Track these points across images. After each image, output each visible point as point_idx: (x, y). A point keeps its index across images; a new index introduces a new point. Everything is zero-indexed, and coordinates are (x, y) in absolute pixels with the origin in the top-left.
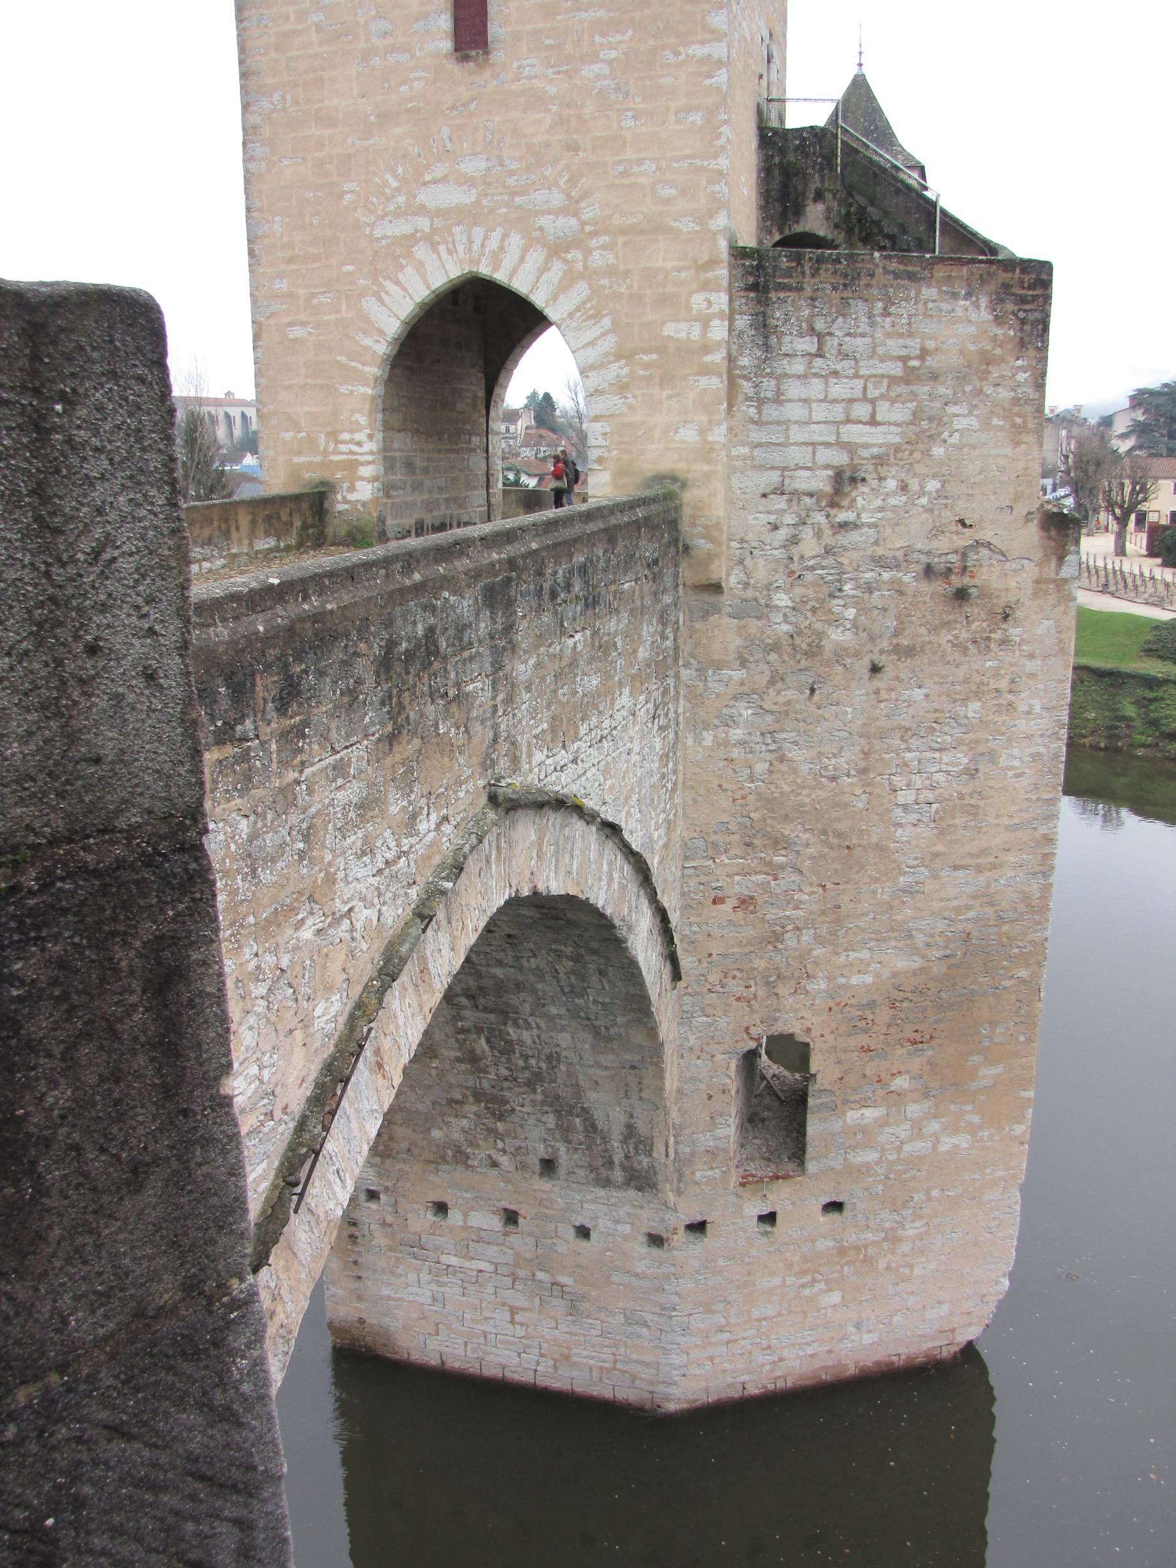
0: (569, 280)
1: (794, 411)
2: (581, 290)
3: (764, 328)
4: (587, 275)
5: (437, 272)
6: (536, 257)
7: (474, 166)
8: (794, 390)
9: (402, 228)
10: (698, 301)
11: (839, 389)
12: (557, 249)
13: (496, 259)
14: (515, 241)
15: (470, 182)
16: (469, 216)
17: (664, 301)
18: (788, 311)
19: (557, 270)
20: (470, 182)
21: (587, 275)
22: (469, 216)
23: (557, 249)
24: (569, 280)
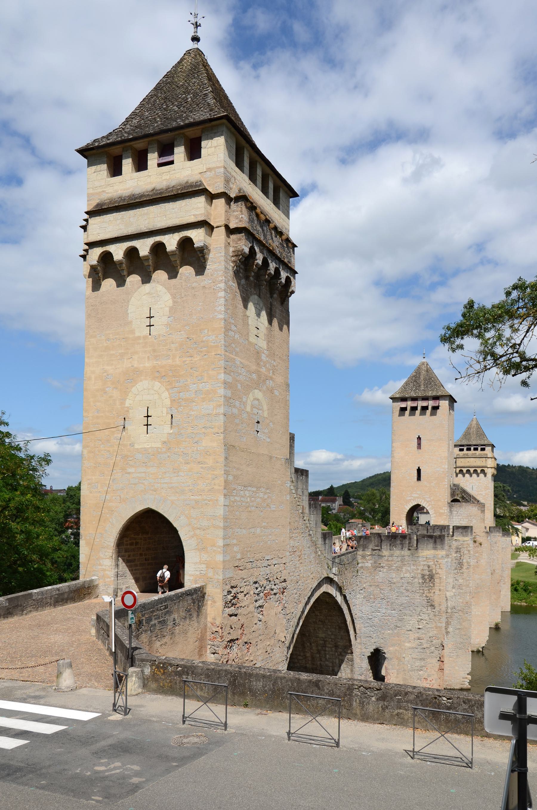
0: (429, 505)
1: (454, 520)
3: (451, 511)
4: (431, 505)
6: (426, 502)
7: (419, 493)
8: (454, 517)
9: (410, 498)
10: (444, 508)
11: (459, 517)
12: (428, 502)
14: (423, 501)
15: (418, 494)
16: (418, 498)
19: (428, 504)
20: (418, 494)
21: (431, 505)
22: (418, 498)
23: (428, 502)
24: (429, 505)
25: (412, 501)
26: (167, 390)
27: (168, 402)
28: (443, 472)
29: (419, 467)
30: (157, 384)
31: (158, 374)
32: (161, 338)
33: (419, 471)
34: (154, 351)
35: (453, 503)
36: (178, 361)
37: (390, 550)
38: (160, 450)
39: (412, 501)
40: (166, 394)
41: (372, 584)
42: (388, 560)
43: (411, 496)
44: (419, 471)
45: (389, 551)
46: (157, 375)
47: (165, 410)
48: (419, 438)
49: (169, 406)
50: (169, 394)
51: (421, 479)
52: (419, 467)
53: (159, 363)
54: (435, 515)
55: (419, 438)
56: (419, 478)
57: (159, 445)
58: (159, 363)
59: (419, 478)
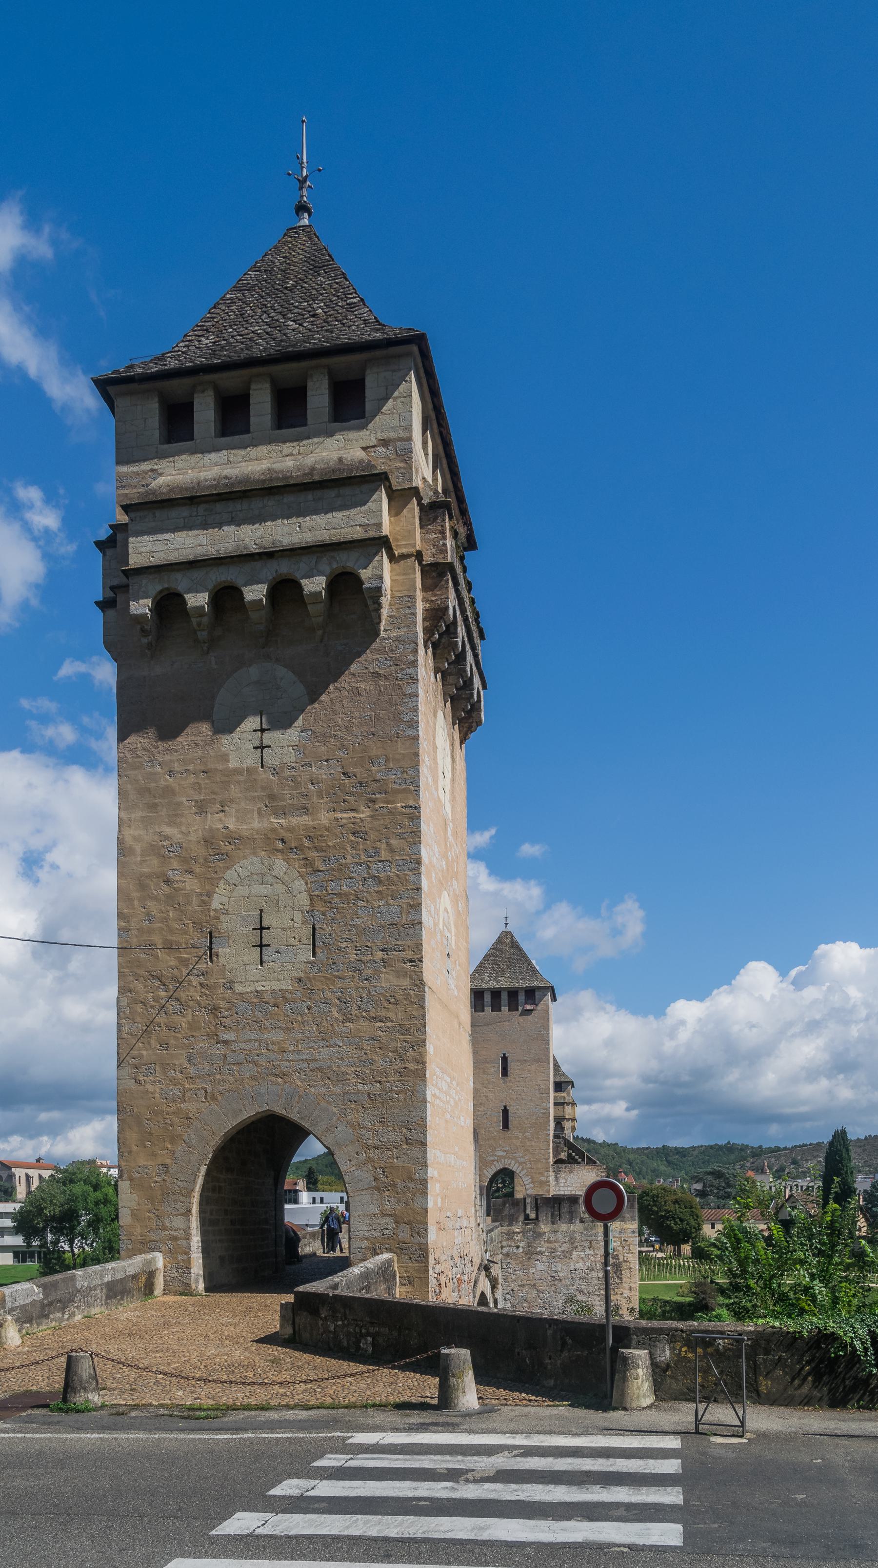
0: (523, 1169)
2: (525, 1171)
5: (500, 1166)
6: (517, 1165)
9: (492, 1158)
12: (520, 1164)
13: (509, 1165)
14: (513, 1162)
16: (504, 1157)
17: (540, 1173)
18: (562, 1175)
19: (520, 1168)
22: (504, 1157)
23: (520, 1164)
24: (523, 1169)
25: (495, 1163)
26: (301, 875)
27: (304, 900)
28: (544, 1113)
29: (505, 1107)
30: (279, 865)
31: (279, 844)
32: (287, 773)
33: (505, 1112)
34: (272, 797)
35: (560, 1166)
36: (324, 818)
37: (553, 1223)
38: (289, 996)
39: (495, 1163)
40: (299, 885)
41: (525, 1282)
42: (549, 1241)
43: (494, 1155)
44: (505, 1112)
45: (550, 1225)
46: (280, 846)
47: (298, 917)
48: (505, 1059)
49: (307, 908)
50: (306, 884)
51: (510, 1126)
52: (505, 1107)
53: (283, 822)
54: (531, 1185)
55: (505, 1059)
56: (506, 1125)
57: (286, 986)
58: (283, 822)
59: (506, 1125)
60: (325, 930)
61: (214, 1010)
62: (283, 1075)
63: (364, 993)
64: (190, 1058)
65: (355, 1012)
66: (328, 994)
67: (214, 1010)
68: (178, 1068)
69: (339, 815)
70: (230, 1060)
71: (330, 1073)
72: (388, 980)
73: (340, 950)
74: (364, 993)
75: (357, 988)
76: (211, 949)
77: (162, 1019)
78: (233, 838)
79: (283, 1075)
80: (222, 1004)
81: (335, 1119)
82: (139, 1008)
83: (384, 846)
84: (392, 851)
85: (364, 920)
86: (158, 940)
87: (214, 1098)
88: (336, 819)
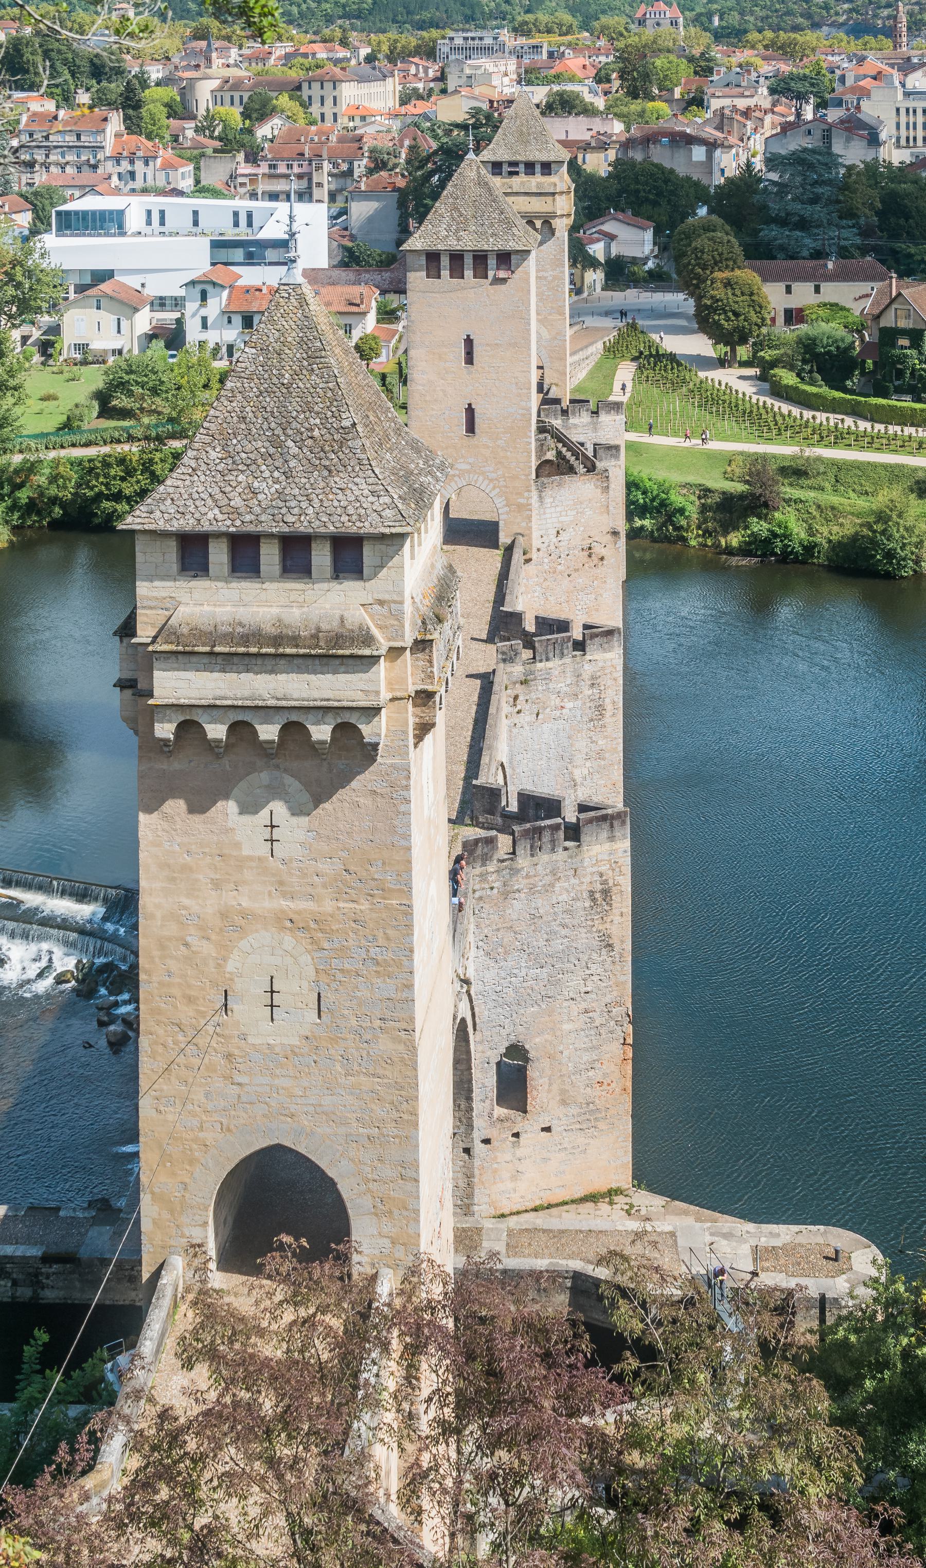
36: (328, 906)
60: (329, 998)
61: (229, 1056)
62: (292, 1116)
63: (364, 1054)
64: (207, 1095)
65: (356, 1068)
66: (332, 1052)
67: (229, 1056)
68: (196, 1103)
69: (341, 905)
70: (244, 1099)
71: (334, 1117)
72: (385, 1045)
73: (343, 1016)
74: (364, 1054)
75: (357, 1049)
76: (226, 1005)
77: (181, 1059)
78: (245, 914)
79: (292, 1116)
80: (236, 1052)
81: (338, 1155)
82: (160, 1049)
83: (381, 934)
84: (388, 939)
85: (363, 993)
86: (176, 991)
87: (229, 1130)
88: (339, 908)
